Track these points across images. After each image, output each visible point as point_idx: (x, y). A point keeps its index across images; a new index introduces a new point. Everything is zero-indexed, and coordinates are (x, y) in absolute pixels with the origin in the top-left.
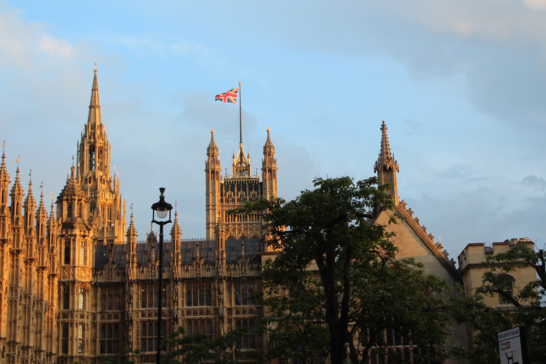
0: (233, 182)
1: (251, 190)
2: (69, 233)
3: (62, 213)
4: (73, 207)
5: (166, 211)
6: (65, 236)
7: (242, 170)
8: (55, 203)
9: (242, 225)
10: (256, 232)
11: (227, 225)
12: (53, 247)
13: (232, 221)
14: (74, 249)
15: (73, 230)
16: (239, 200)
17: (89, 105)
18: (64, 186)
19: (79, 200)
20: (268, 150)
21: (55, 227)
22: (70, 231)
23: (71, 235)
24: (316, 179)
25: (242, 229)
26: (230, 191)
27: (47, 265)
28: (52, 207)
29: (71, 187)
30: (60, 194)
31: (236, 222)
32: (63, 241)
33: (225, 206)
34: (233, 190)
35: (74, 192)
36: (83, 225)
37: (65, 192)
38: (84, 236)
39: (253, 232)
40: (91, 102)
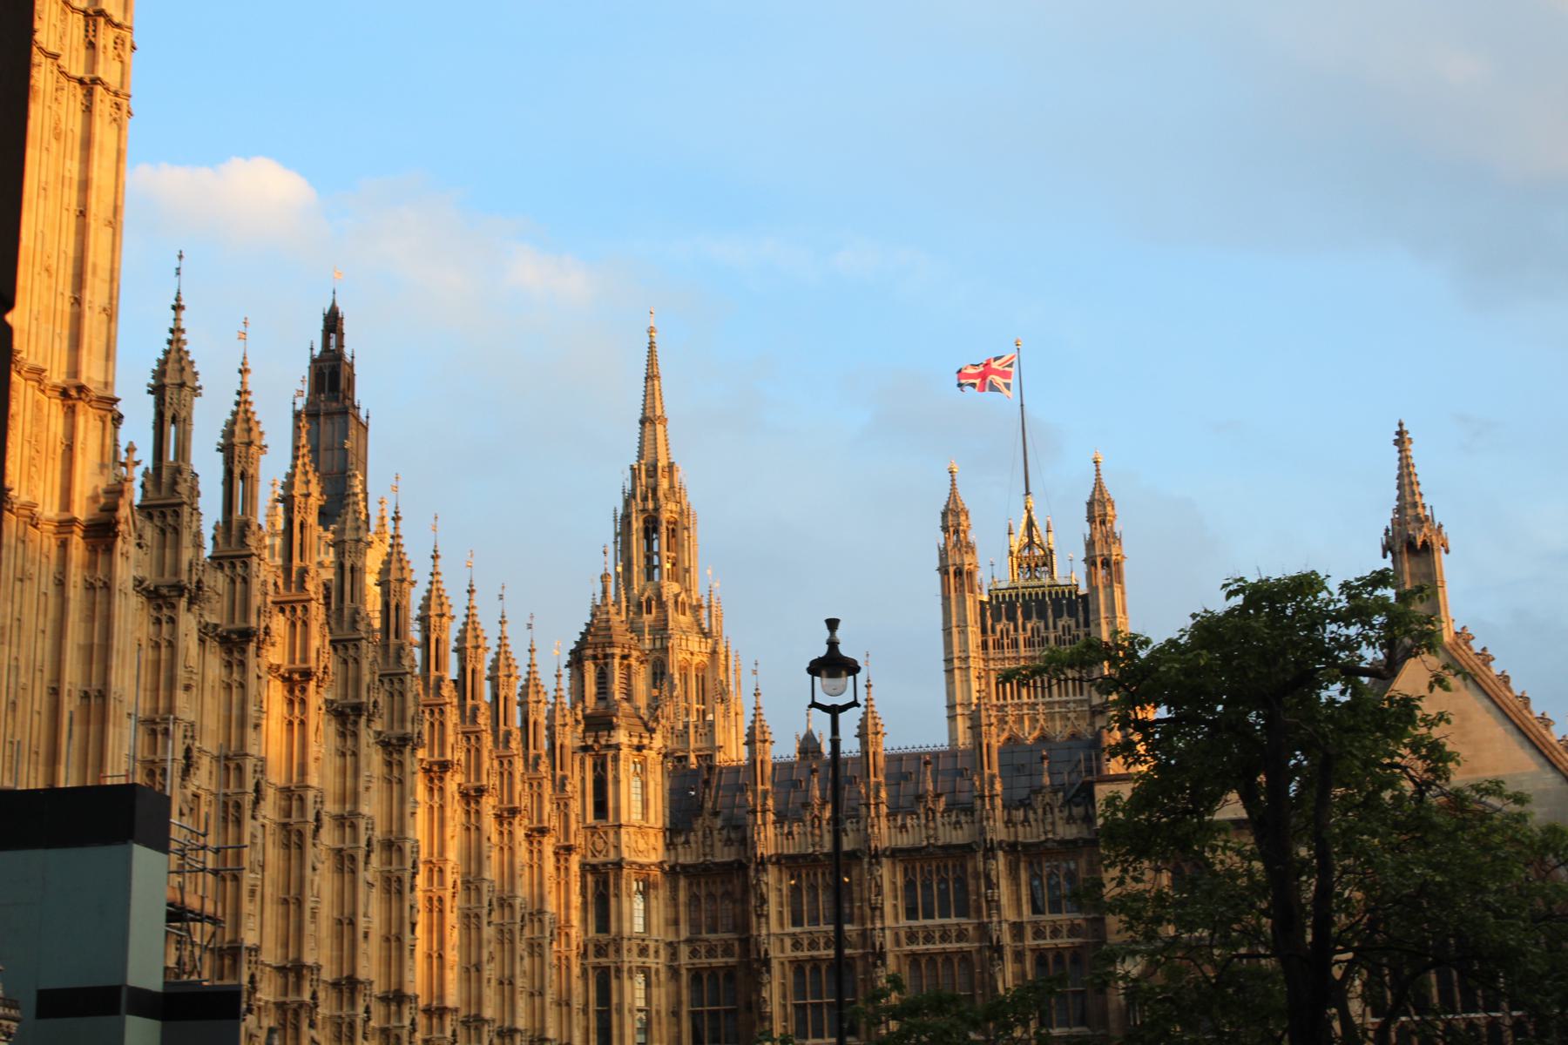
0: (1010, 596)
1: (1058, 615)
2: (603, 742)
3: (583, 691)
4: (610, 676)
5: (843, 679)
6: (594, 750)
7: (1033, 565)
8: (566, 666)
9: (1040, 708)
10: (1076, 723)
11: (1001, 708)
12: (564, 778)
13: (1012, 698)
14: (617, 781)
15: (612, 733)
16: (1029, 643)
17: (639, 416)
18: (587, 624)
19: (624, 657)
20: (1098, 510)
21: (567, 728)
22: (603, 736)
23: (609, 746)
24: (1230, 581)
25: (1041, 718)
26: (1004, 620)
27: (552, 824)
28: (558, 676)
29: (603, 624)
30: (576, 642)
31: (1025, 699)
32: (589, 762)
33: (993, 659)
34: (1012, 617)
35: (611, 637)
36: (637, 721)
37: (589, 638)
38: (640, 748)
39: (1069, 723)
40: (644, 409)
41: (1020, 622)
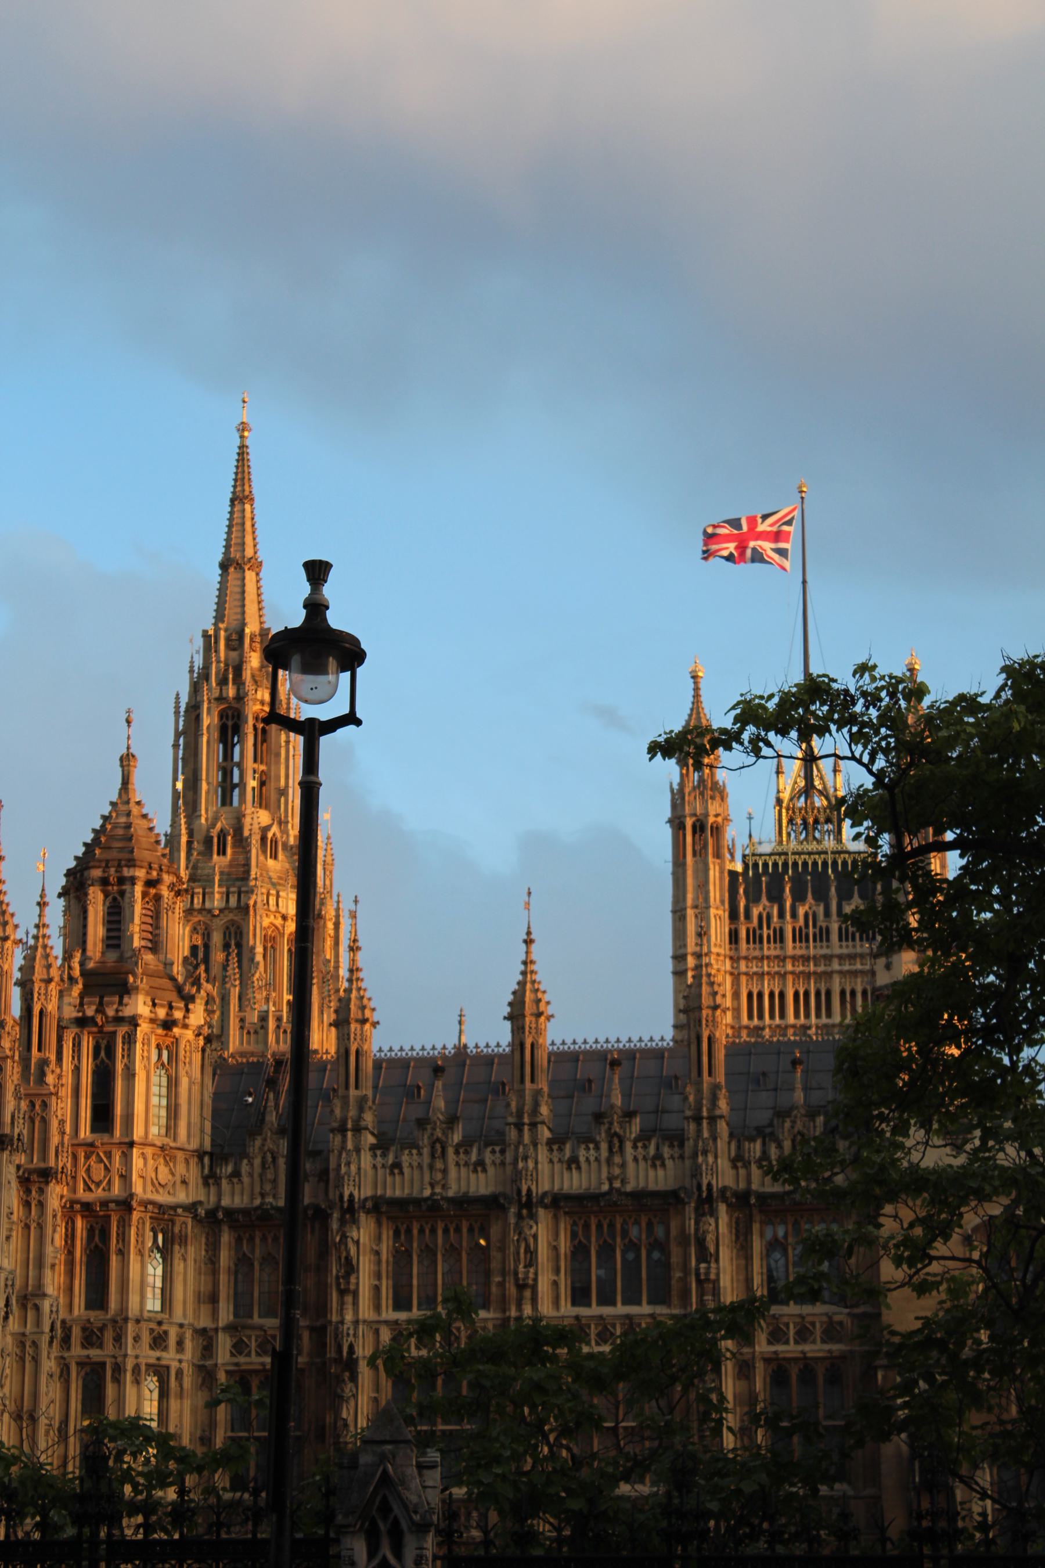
0: (775, 865)
2: (110, 1012)
3: (85, 934)
4: (127, 913)
5: (331, 677)
6: (96, 1024)
7: (811, 820)
8: (60, 895)
12: (44, 1063)
13: (772, 1016)
14: (130, 1075)
15: (126, 1000)
16: (800, 936)
17: (219, 557)
18: (94, 831)
19: (150, 883)
21: (52, 985)
22: (113, 1003)
23: (119, 1020)
26: (764, 900)
27: (17, 1131)
28: (42, 904)
29: (120, 832)
30: (76, 858)
31: (791, 1019)
32: (87, 1044)
34: (776, 897)
35: (132, 852)
36: (166, 983)
37: (97, 852)
38: (168, 1025)
40: (227, 547)
41: (788, 904)
